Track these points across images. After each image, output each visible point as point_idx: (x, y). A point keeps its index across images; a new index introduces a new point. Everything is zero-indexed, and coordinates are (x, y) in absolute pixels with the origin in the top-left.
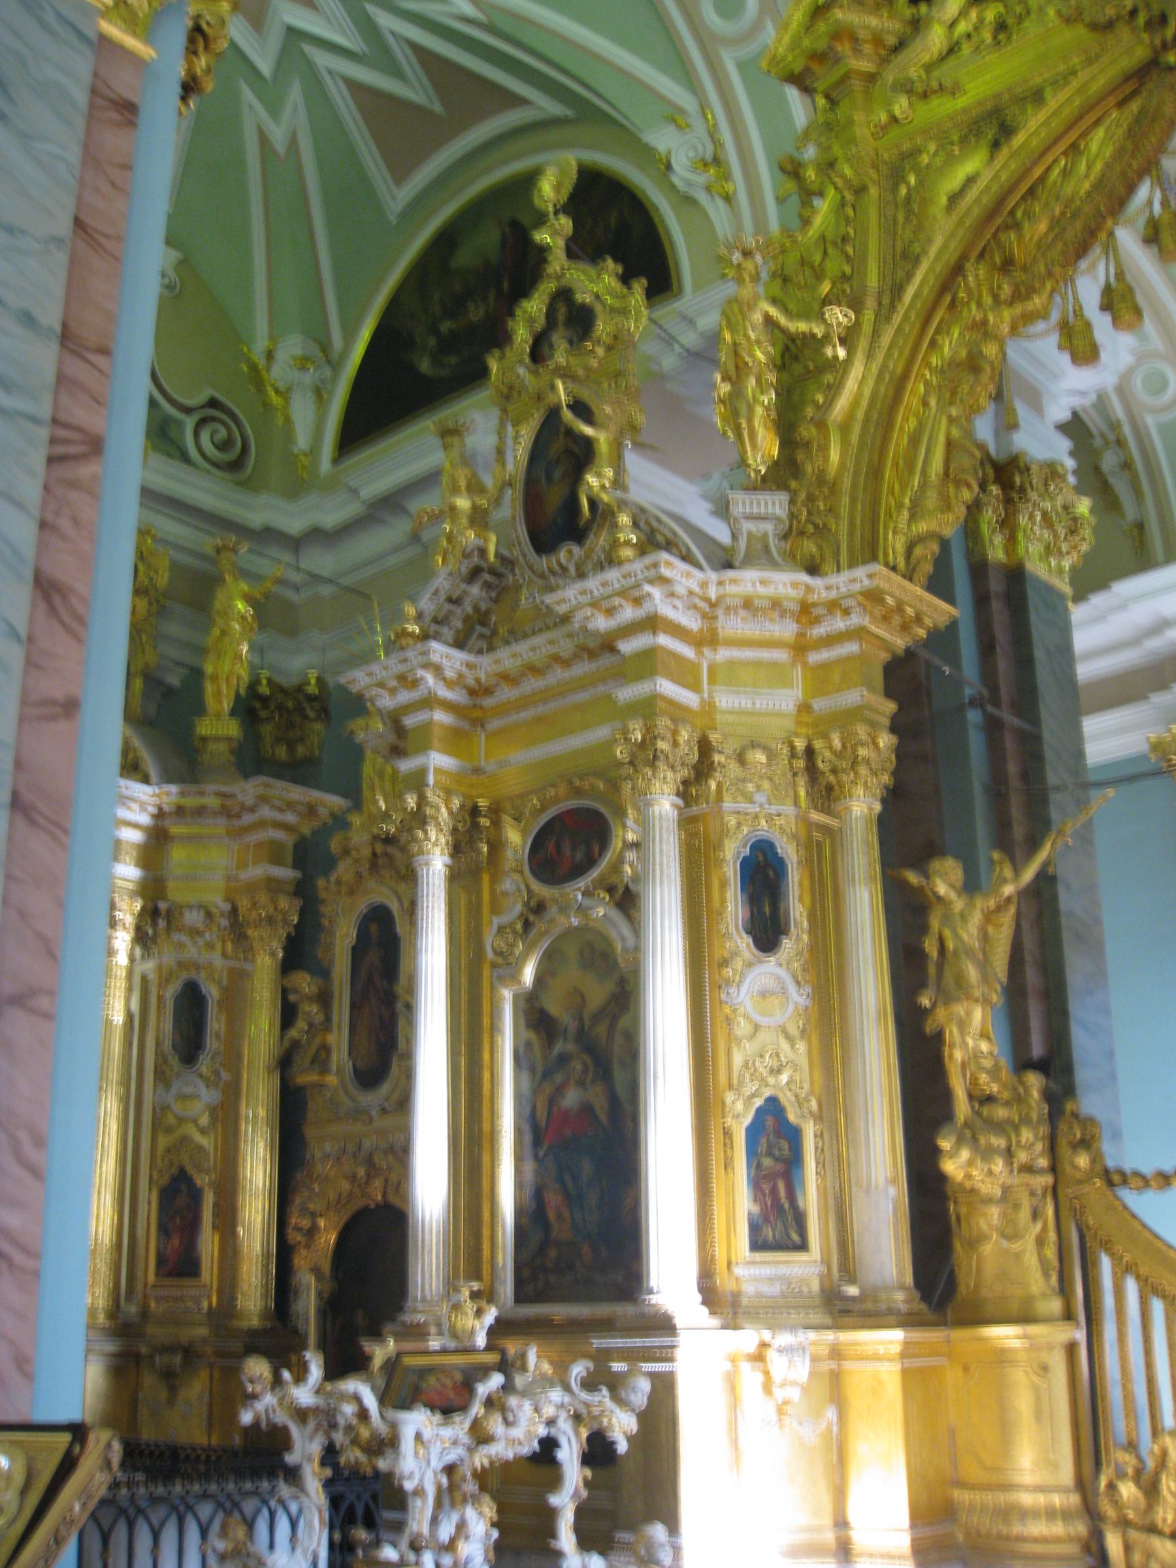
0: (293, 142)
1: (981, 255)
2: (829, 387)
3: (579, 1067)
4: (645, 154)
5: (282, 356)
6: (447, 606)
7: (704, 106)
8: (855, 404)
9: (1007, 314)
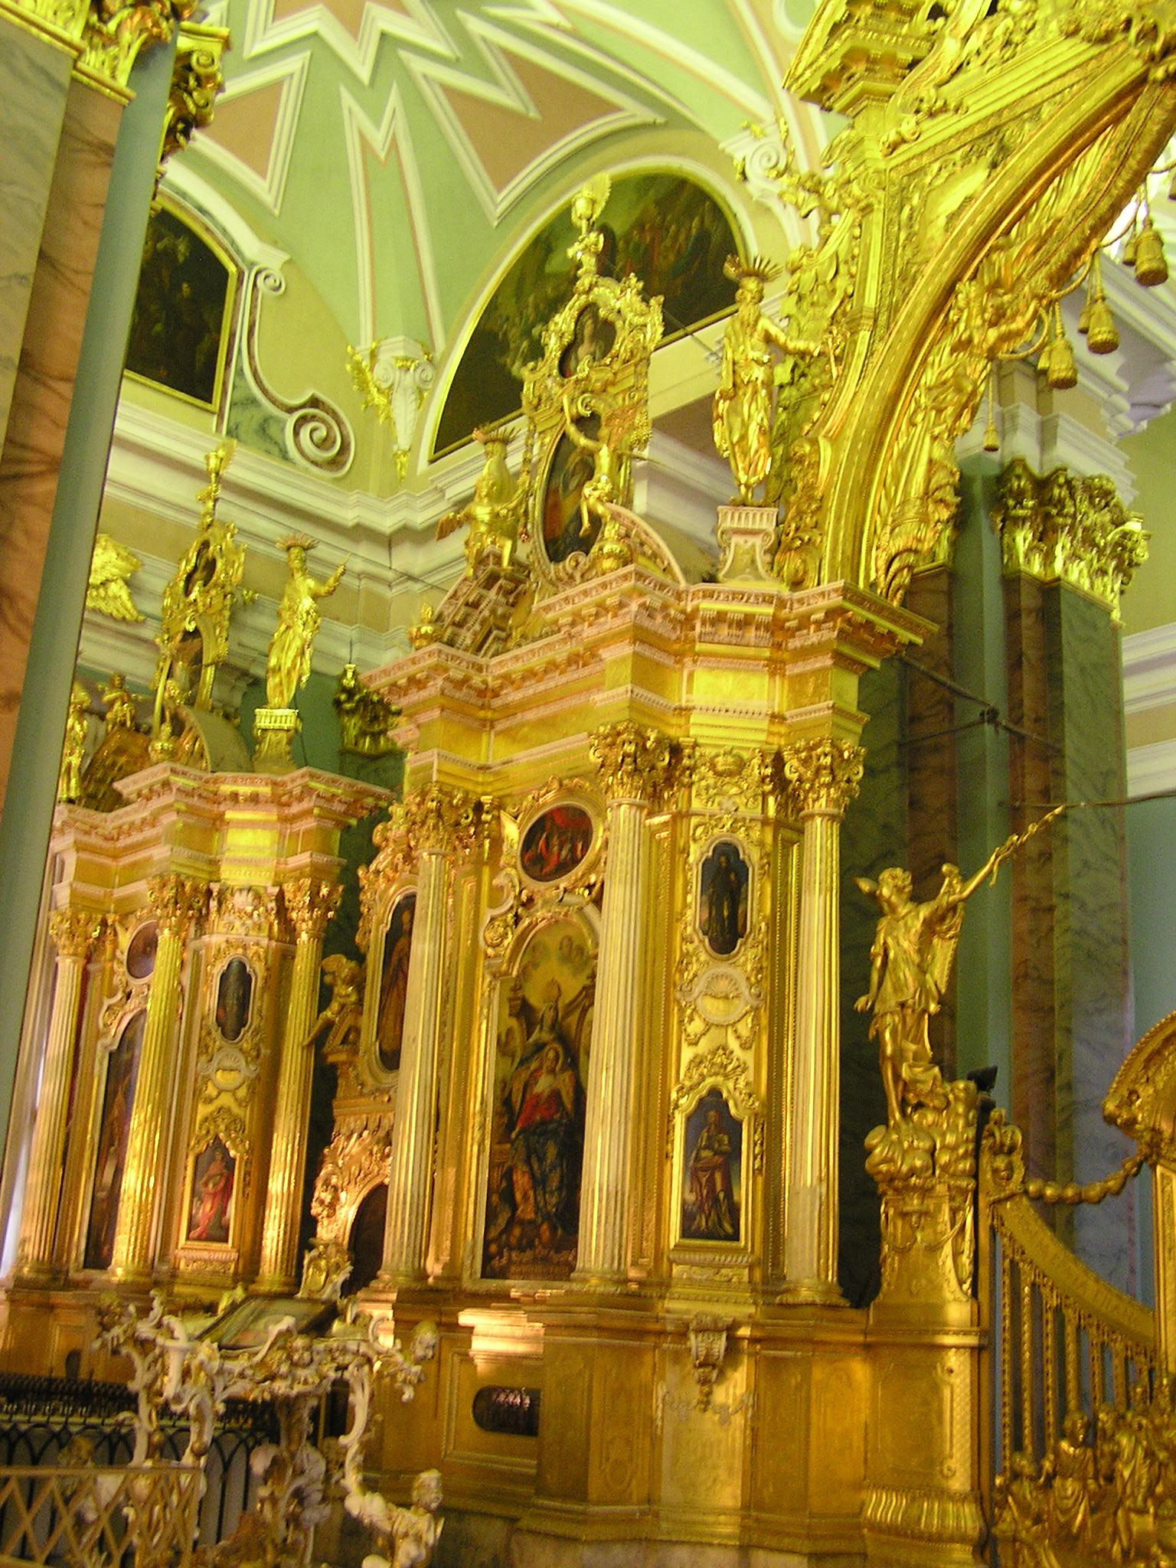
0: (394, 145)
1: (974, 277)
3: (551, 1054)
4: (721, 161)
5: (383, 357)
6: (463, 610)
7: (778, 115)
9: (993, 334)
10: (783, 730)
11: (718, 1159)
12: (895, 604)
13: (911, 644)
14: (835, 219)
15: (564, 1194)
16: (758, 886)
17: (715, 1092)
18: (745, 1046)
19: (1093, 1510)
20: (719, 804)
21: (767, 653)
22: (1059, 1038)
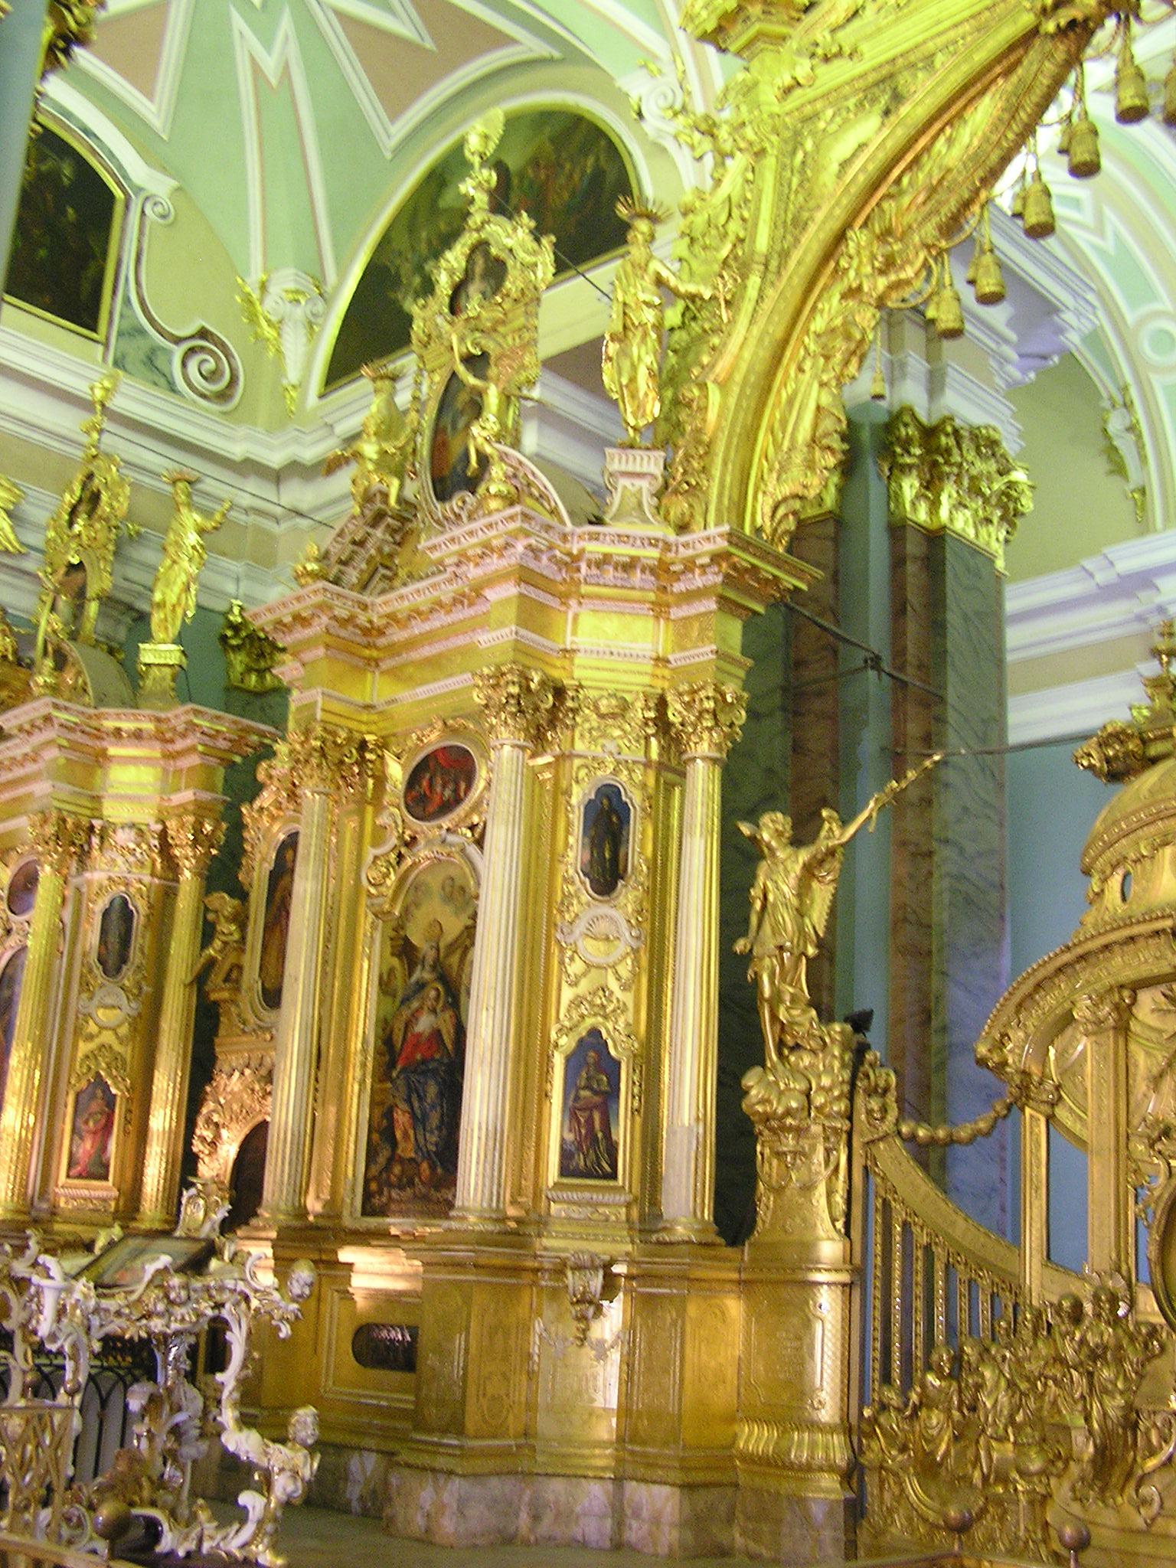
0: (286, 72)
1: (865, 225)
2: (714, 349)
3: (433, 994)
4: (618, 99)
5: (274, 289)
6: (351, 547)
7: (675, 52)
8: (734, 367)
9: (882, 283)
10: (666, 673)
12: (781, 550)
13: (797, 589)
14: (729, 162)
15: (444, 1132)
16: (639, 827)
17: (595, 1033)
18: (625, 988)
19: (956, 1439)
20: (603, 746)
21: (652, 596)
22: (935, 982)
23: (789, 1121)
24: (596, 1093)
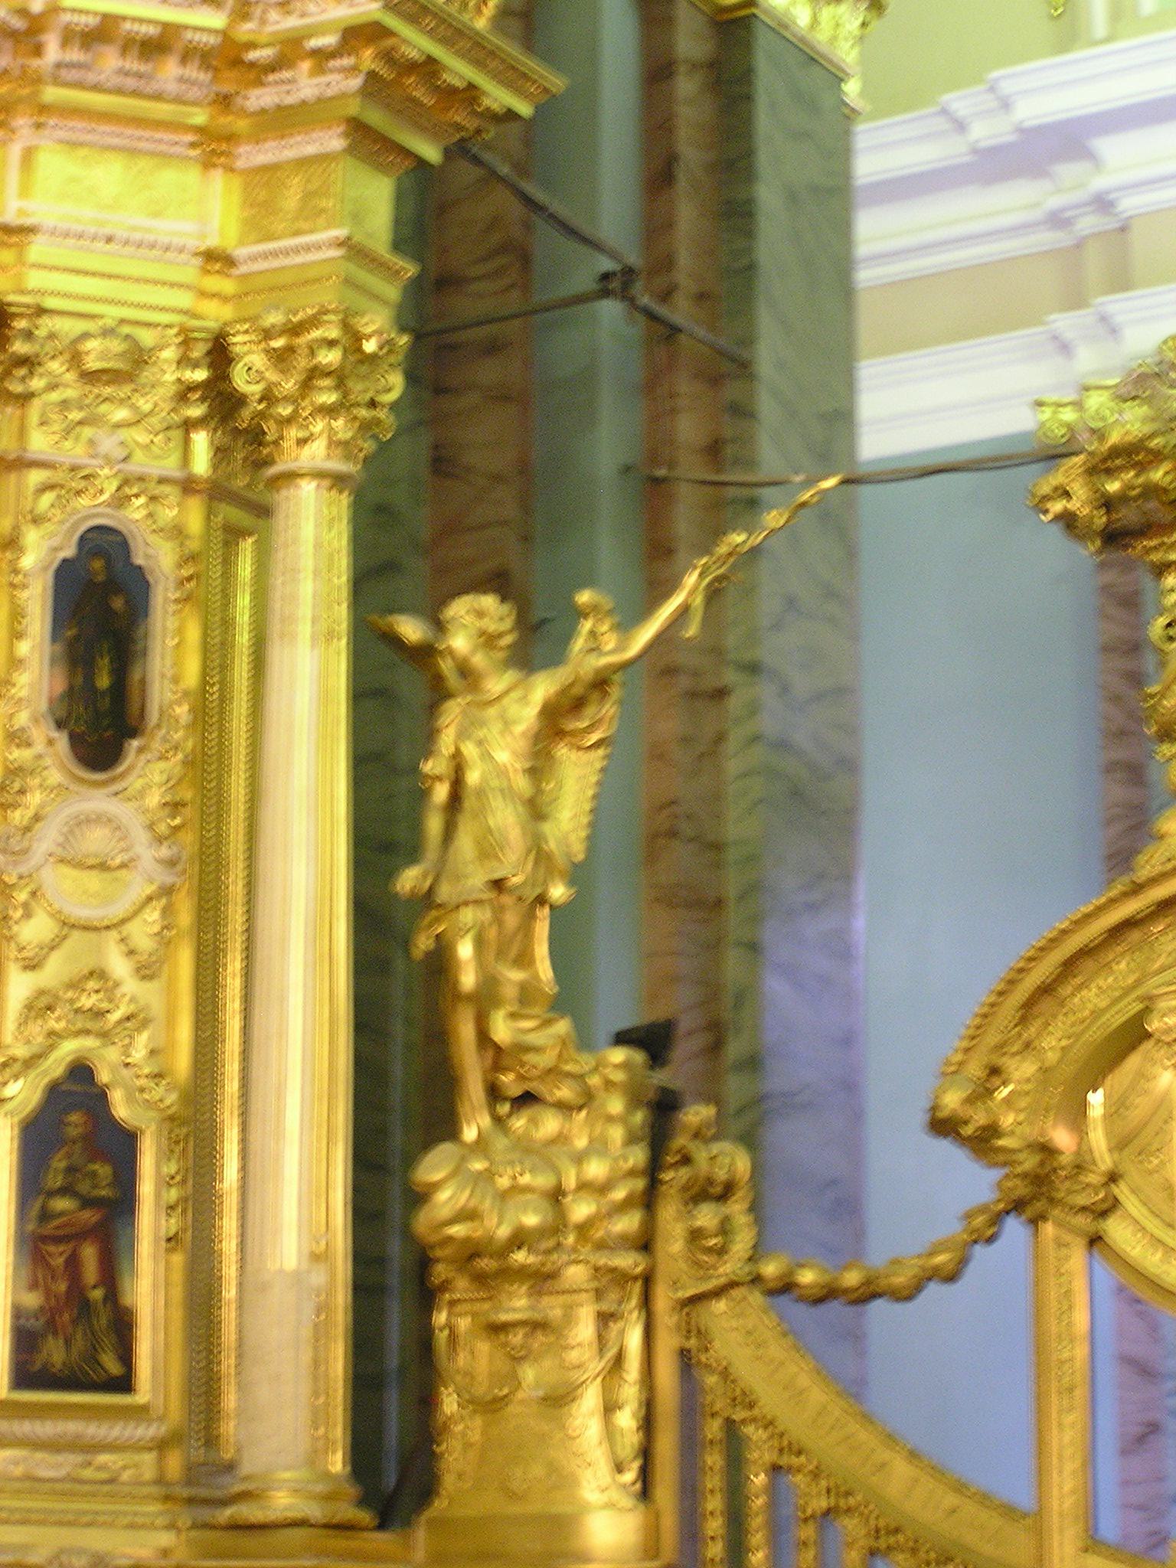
10: (227, 286)
11: (89, 1216)
12: (481, 24)
13: (511, 115)
16: (172, 623)
17: (81, 1071)
18: (146, 972)
20: (91, 442)
21: (199, 117)
22: (733, 965)
23: (520, 1257)
24: (87, 1203)
